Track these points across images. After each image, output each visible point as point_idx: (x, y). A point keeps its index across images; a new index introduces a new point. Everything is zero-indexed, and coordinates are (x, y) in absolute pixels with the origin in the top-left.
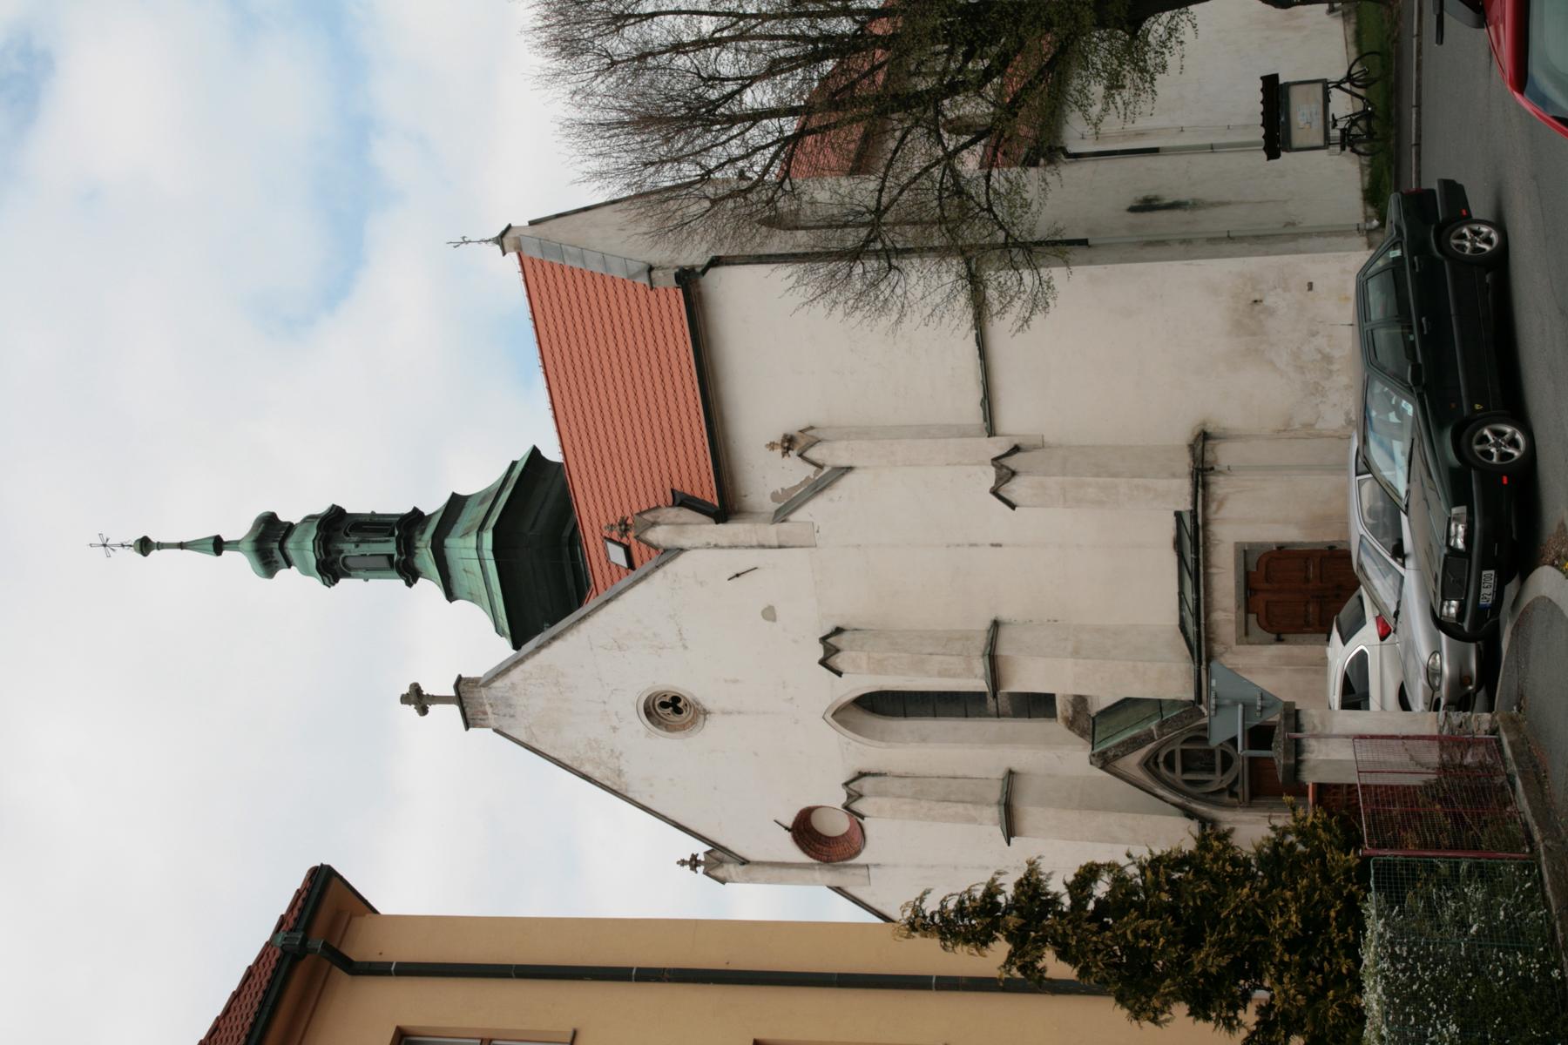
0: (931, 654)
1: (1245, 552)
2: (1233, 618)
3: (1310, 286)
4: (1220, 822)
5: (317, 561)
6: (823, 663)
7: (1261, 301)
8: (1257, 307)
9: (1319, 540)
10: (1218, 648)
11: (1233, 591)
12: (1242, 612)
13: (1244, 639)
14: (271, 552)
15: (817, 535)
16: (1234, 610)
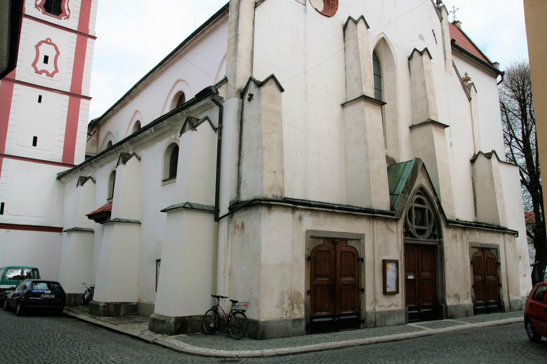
0: (435, 99)
1: (496, 249)
2: (477, 242)
3: (525, 276)
4: (397, 224)
6: (415, 50)
7: (520, 259)
8: (519, 258)
9: (502, 281)
10: (467, 232)
11: (485, 243)
12: (479, 246)
13: (471, 246)
15: (449, 75)
16: (480, 242)
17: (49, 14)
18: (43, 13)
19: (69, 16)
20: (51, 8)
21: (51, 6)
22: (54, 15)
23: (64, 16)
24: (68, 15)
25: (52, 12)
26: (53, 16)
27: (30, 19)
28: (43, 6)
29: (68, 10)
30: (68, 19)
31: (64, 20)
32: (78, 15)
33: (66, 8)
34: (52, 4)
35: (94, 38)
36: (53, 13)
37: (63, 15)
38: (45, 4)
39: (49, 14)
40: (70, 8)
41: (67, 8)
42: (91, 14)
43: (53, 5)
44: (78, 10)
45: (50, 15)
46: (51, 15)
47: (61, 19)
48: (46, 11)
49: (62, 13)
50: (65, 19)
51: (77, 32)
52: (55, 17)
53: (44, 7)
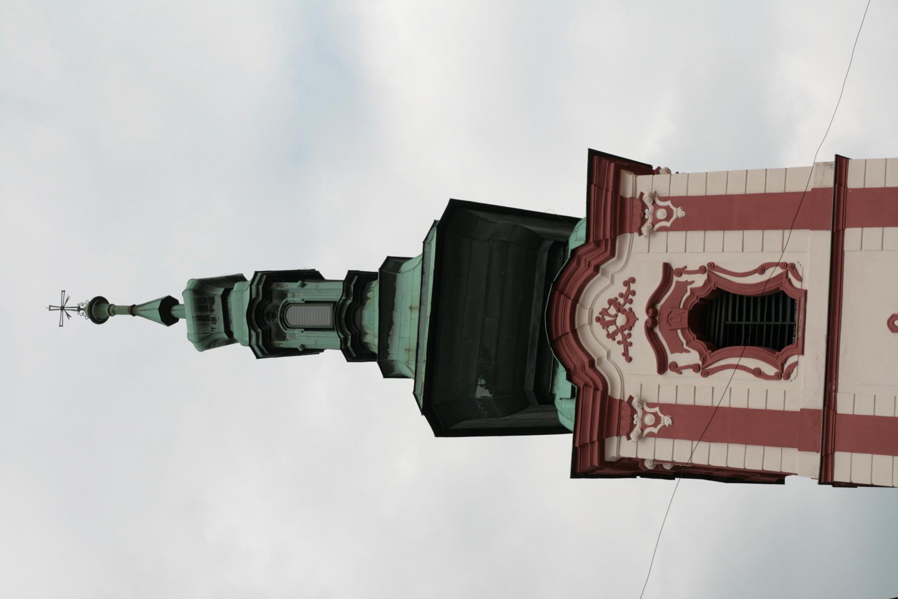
5: (252, 302)
14: (212, 301)
17: (800, 333)
18: (803, 353)
19: (785, 265)
20: (776, 326)
21: (769, 326)
22: (799, 317)
23: (790, 281)
24: (782, 268)
25: (788, 322)
26: (801, 317)
27: (836, 391)
28: (777, 353)
29: (762, 270)
30: (797, 266)
31: (804, 278)
32: (773, 236)
33: (757, 279)
34: (761, 326)
35: (841, 163)
36: (792, 319)
37: (787, 284)
38: (767, 345)
39: (800, 333)
40: (756, 266)
41: (757, 275)
42: (755, 188)
43: (762, 320)
44: (753, 236)
45: (801, 329)
46: (801, 325)
47: (806, 292)
48: (790, 342)
49: (781, 289)
50: (800, 279)
51: (838, 231)
52: (802, 311)
53: (780, 351)
